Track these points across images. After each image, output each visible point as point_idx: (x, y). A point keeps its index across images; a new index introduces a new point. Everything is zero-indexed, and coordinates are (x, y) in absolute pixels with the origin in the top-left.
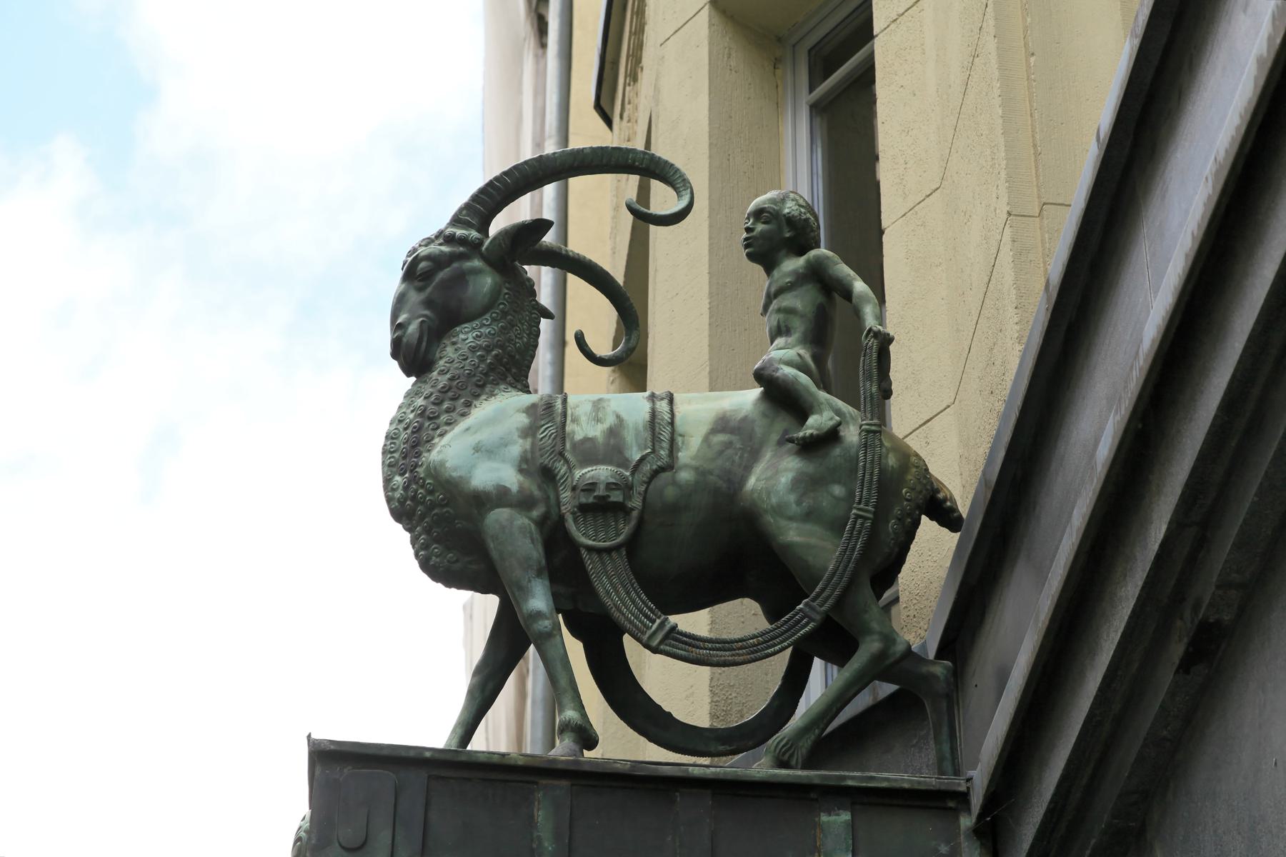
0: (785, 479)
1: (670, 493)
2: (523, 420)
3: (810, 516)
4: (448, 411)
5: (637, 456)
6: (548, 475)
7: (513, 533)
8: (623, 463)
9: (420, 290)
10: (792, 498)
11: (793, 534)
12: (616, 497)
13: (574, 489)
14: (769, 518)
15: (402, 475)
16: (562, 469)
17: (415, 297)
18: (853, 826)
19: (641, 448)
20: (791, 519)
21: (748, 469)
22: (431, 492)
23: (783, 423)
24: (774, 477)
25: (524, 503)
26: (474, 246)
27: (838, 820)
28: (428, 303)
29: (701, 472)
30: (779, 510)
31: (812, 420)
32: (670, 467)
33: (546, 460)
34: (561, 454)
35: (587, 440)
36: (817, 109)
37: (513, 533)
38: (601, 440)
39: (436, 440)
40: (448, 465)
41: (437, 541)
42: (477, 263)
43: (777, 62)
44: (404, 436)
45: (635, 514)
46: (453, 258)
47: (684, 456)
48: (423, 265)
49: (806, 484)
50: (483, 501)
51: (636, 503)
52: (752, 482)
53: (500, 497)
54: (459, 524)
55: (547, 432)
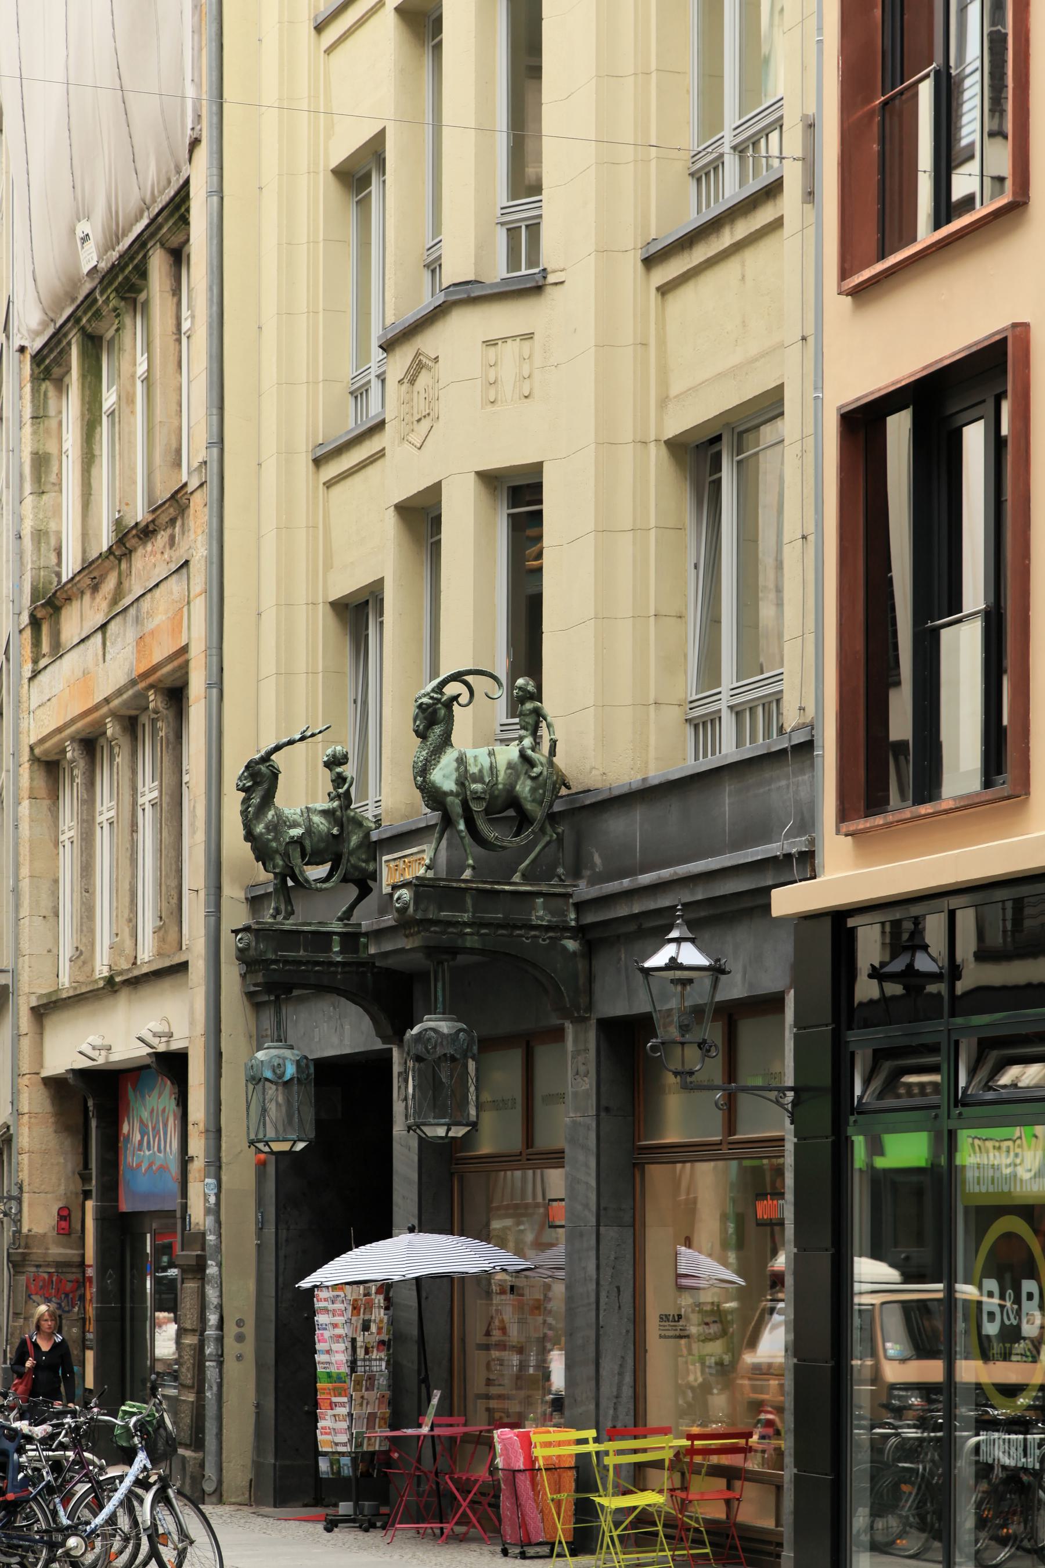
0: (527, 789)
1: (496, 792)
2: (455, 764)
3: (533, 801)
7: (455, 804)
8: (483, 783)
11: (529, 806)
12: (483, 796)
17: (421, 715)
18: (543, 902)
21: (516, 783)
23: (526, 767)
24: (524, 788)
25: (457, 795)
26: (439, 700)
28: (425, 718)
29: (504, 785)
30: (525, 799)
32: (496, 784)
33: (462, 780)
36: (508, 515)
37: (455, 804)
42: (440, 706)
43: (495, 489)
44: (420, 764)
46: (434, 704)
47: (500, 779)
49: (533, 790)
50: (446, 794)
51: (487, 797)
52: (518, 787)
53: (451, 793)
55: (462, 769)
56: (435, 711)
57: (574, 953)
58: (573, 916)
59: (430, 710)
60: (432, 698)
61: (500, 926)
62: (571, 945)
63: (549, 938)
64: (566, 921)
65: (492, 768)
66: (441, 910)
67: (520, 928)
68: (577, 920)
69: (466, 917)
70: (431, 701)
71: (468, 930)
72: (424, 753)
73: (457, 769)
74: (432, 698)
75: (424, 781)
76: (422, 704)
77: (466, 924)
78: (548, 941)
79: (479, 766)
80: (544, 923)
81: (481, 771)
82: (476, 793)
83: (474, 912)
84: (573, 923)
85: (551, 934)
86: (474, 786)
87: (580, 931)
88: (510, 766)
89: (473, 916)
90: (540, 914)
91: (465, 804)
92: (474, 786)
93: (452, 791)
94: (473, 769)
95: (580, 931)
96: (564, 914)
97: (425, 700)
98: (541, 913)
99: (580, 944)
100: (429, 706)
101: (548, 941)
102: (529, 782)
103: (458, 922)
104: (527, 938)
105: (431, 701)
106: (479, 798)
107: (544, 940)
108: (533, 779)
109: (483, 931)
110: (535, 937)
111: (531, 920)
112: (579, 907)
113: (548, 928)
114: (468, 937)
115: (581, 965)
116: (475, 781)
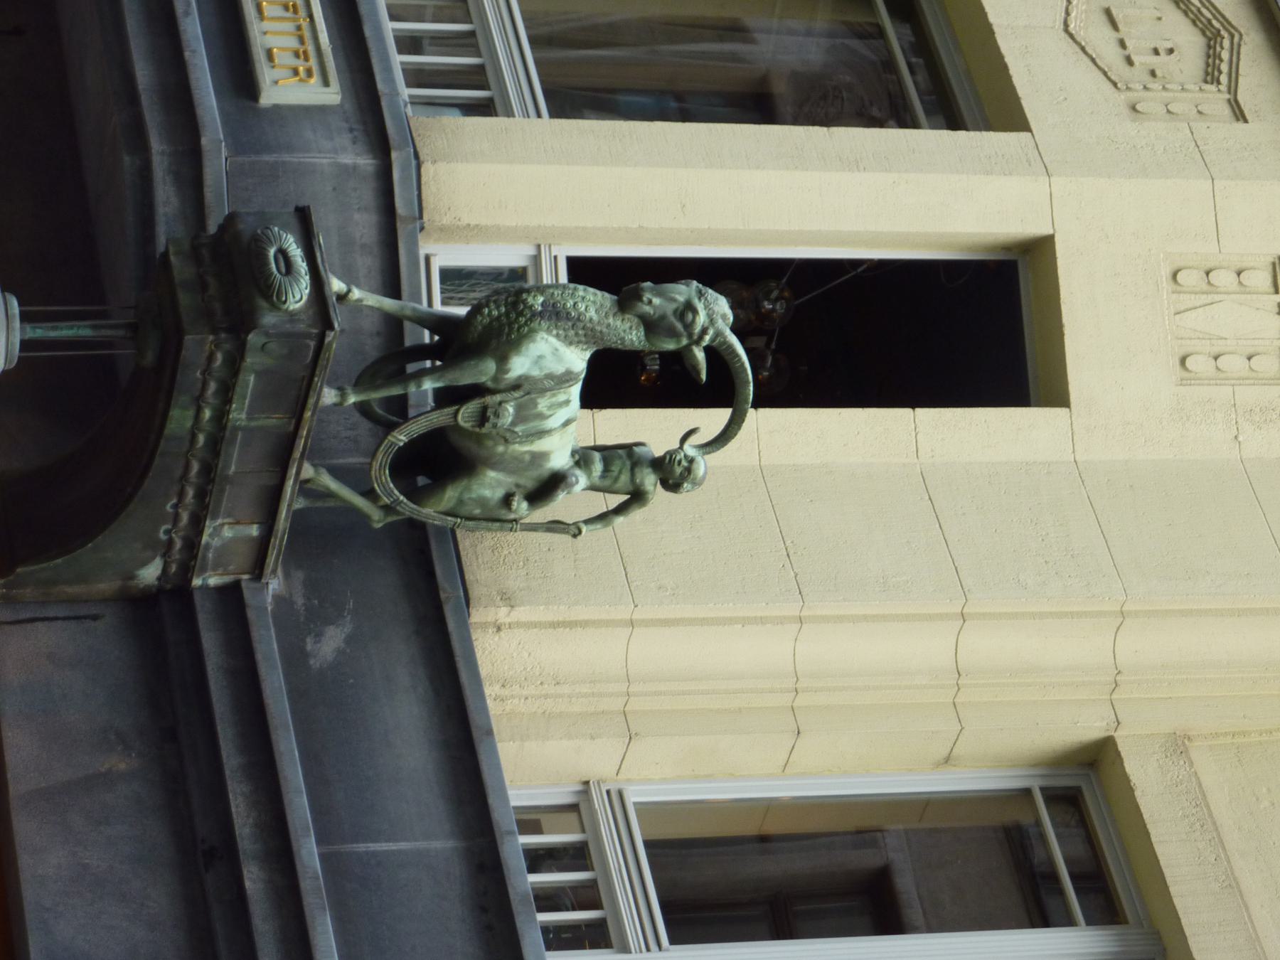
0: (487, 493)
3: (460, 502)
4: (577, 334)
5: (517, 429)
6: (516, 386)
8: (514, 424)
9: (675, 312)
10: (474, 496)
11: (450, 495)
13: (500, 403)
14: (464, 483)
15: (542, 305)
16: (516, 394)
19: (523, 431)
20: (461, 493)
22: (519, 328)
27: (254, 531)
30: (468, 489)
31: (525, 505)
33: (526, 387)
34: (528, 393)
35: (536, 405)
38: (535, 411)
39: (555, 332)
40: (532, 345)
41: (491, 322)
42: (685, 342)
44: (570, 304)
45: (477, 430)
48: (690, 316)
50: (503, 360)
52: (492, 474)
54: (494, 343)
55: (547, 383)
56: (673, 334)
57: (133, 577)
58: (213, 581)
59: (679, 326)
60: (704, 331)
61: (208, 471)
62: (150, 573)
63: (170, 543)
64: (203, 570)
65: (542, 434)
66: (259, 374)
67: (202, 495)
68: (204, 588)
69: (238, 415)
70: (698, 329)
71: (207, 414)
72: (592, 313)
73: (550, 376)
74: (704, 331)
75: (534, 315)
76: (695, 312)
77: (221, 416)
78: (163, 537)
79: (549, 413)
80: (205, 538)
81: (542, 417)
82: (497, 415)
83: (244, 429)
84: (197, 582)
85: (178, 544)
86: (510, 409)
87: (176, 592)
88: (539, 458)
89: (236, 429)
90: (227, 532)
91: (477, 391)
92: (510, 409)
93: (507, 372)
94: (543, 404)
95: (176, 592)
96: (218, 566)
97: (702, 319)
98: (228, 533)
99: (148, 587)
100: (689, 327)
101: (163, 537)
102: (499, 493)
103: (230, 401)
104: (176, 506)
105: (698, 329)
106: (482, 418)
107: (168, 532)
108: (507, 500)
109: (201, 439)
110: (176, 518)
111: (215, 517)
112: (231, 596)
113: (192, 545)
114: (191, 413)
115: (107, 586)
116: (519, 409)
